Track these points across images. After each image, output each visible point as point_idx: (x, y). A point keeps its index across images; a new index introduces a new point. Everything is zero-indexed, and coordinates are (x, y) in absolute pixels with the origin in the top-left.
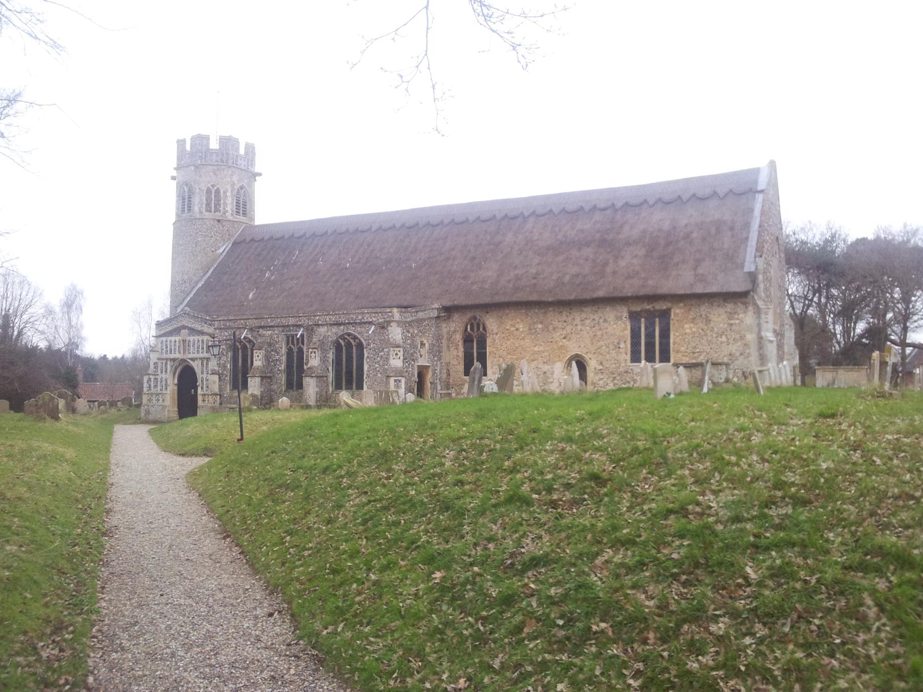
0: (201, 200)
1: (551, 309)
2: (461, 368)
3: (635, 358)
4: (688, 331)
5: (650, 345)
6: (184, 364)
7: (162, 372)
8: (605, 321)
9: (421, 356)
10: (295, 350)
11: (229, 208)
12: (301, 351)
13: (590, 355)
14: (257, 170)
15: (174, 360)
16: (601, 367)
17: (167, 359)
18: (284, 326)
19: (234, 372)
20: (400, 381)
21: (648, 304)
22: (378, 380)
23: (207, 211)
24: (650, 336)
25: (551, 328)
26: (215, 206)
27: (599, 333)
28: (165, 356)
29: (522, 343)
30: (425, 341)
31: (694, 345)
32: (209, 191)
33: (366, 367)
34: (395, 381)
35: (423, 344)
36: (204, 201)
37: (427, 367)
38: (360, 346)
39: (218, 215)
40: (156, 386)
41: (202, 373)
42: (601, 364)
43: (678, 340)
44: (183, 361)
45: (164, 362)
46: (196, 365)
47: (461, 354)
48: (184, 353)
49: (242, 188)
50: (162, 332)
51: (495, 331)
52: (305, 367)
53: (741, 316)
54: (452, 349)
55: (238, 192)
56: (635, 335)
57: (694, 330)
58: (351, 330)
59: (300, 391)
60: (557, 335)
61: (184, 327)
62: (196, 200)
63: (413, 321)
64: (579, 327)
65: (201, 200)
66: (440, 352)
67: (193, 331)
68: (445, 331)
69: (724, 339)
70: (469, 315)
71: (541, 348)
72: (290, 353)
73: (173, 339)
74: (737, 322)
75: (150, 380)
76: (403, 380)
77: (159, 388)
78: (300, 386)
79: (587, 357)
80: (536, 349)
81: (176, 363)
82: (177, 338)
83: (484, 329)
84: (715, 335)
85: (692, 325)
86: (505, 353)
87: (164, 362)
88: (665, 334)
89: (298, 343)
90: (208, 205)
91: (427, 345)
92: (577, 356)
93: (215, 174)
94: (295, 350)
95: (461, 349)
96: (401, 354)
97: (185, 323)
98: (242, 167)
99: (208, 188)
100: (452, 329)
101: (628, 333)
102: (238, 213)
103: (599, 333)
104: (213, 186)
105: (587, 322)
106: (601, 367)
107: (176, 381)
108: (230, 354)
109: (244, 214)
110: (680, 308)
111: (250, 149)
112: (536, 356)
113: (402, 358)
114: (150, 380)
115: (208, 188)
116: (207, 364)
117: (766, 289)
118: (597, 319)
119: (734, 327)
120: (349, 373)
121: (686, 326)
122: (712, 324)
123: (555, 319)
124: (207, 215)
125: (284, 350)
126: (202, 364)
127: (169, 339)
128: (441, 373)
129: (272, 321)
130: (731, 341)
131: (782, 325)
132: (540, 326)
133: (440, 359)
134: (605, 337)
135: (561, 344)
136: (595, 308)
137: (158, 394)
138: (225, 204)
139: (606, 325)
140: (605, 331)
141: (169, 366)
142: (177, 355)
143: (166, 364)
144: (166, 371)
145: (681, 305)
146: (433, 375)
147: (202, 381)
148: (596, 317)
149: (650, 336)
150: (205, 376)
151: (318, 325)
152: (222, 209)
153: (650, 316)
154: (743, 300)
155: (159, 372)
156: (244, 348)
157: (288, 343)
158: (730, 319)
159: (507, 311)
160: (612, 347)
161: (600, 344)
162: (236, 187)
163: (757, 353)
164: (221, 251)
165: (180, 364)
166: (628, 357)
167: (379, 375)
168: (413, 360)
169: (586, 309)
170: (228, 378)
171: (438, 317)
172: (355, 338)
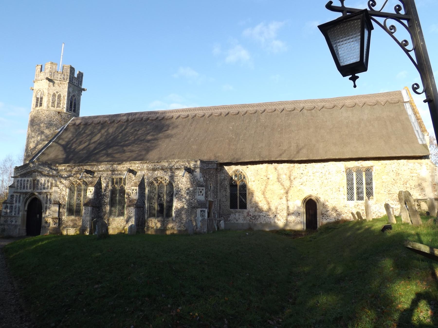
0: (49, 100)
2: (228, 203)
3: (351, 198)
6: (33, 197)
7: (16, 202)
11: (65, 106)
14: (83, 87)
15: (26, 193)
17: (20, 193)
20: (204, 211)
23: (52, 106)
24: (360, 183)
26: (58, 104)
31: (389, 189)
32: (54, 95)
34: (201, 211)
36: (51, 101)
45: (18, 194)
47: (228, 194)
48: (34, 189)
49: (74, 96)
54: (222, 191)
55: (72, 98)
65: (49, 100)
66: (217, 193)
82: (30, 179)
87: (18, 194)
90: (53, 103)
93: (59, 85)
95: (228, 190)
98: (75, 84)
99: (54, 94)
100: (223, 178)
104: (57, 92)
107: (26, 208)
109: (74, 111)
111: (81, 75)
113: (204, 194)
115: (54, 94)
122: (400, 176)
133: (217, 197)
138: (64, 103)
141: (21, 198)
142: (29, 190)
143: (20, 196)
144: (19, 201)
149: (360, 183)
152: (61, 106)
153: (359, 171)
155: (14, 202)
158: (411, 173)
162: (71, 95)
165: (30, 197)
166: (346, 197)
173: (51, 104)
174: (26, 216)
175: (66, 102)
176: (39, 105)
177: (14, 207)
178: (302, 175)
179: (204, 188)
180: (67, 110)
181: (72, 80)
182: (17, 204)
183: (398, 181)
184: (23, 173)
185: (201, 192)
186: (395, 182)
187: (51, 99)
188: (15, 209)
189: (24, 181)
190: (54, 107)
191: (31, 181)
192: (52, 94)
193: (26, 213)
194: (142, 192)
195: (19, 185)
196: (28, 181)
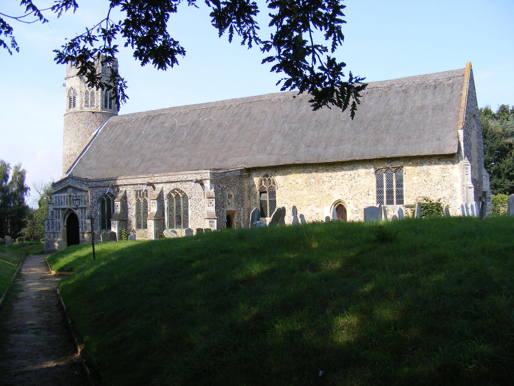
0: (82, 99)
1: (321, 168)
4: (415, 182)
5: (390, 192)
6: (70, 212)
7: (56, 218)
8: (359, 176)
9: (229, 204)
10: (142, 201)
11: (99, 104)
12: (146, 202)
13: (348, 201)
15: (63, 209)
16: (356, 209)
17: (59, 209)
18: (134, 185)
19: (102, 217)
21: (388, 164)
22: (199, 221)
23: (86, 106)
24: (390, 185)
25: (321, 181)
26: (91, 103)
27: (355, 184)
28: (58, 207)
29: (301, 192)
30: (232, 193)
31: (419, 191)
33: (190, 212)
35: (230, 196)
37: (233, 213)
38: (185, 197)
39: (93, 109)
40: (53, 228)
41: (82, 218)
42: (357, 206)
43: (408, 189)
44: (70, 210)
46: (77, 212)
50: (56, 190)
51: (282, 185)
52: (149, 213)
53: (450, 170)
54: (252, 198)
56: (379, 185)
57: (419, 181)
58: (179, 186)
59: (146, 230)
60: (325, 187)
61: (70, 187)
62: (78, 99)
63: (222, 178)
64: (341, 181)
65: (82, 99)
67: (75, 188)
68: (246, 185)
69: (439, 187)
70: (264, 173)
71: (314, 197)
72: (138, 204)
73: (63, 195)
74: (448, 174)
75: (49, 223)
76: (216, 221)
77: (55, 229)
78: (146, 227)
79: (346, 202)
80: (311, 197)
81: (65, 211)
82: (66, 195)
83: (274, 183)
84: (433, 185)
85: (418, 178)
86: (289, 200)
88: (400, 184)
89: (143, 196)
90: (86, 102)
91: (233, 196)
92: (339, 201)
94: (142, 201)
96: (214, 203)
97: (70, 184)
99: (87, 91)
101: (374, 184)
102: (106, 107)
103: (355, 184)
105: (346, 177)
106: (356, 209)
107: (65, 224)
108: (99, 205)
110: (410, 165)
112: (311, 202)
114: (49, 223)
116: (85, 212)
117: (466, 152)
118: (353, 175)
119: (446, 178)
120: (178, 217)
121: (414, 178)
122: (431, 177)
123: (324, 175)
124: (87, 109)
125: (134, 201)
126: (82, 212)
127: (60, 195)
128: (243, 215)
129: (126, 182)
130: (444, 188)
131: (480, 176)
132: (313, 180)
133: (243, 206)
134: (359, 187)
135: (328, 193)
136: (351, 167)
137: (54, 233)
138: (97, 100)
139: (359, 179)
140: (358, 183)
141: (60, 214)
142: (66, 206)
143: (59, 212)
144: (59, 217)
145: (410, 163)
146: (238, 217)
147: (82, 224)
148: (352, 172)
149: (390, 185)
150: (83, 220)
151: (157, 183)
152: (95, 104)
154: (452, 159)
155: (55, 218)
156: (109, 200)
157: (137, 197)
159: (290, 170)
160: (363, 194)
161: (356, 192)
163: (461, 197)
164: (95, 133)
165: (68, 212)
167: (199, 218)
168: (223, 207)
169: (345, 168)
170: (98, 222)
171: (241, 176)
172: (181, 192)
173: (84, 103)
174: (66, 231)
175: (100, 100)
176: (72, 106)
177: (55, 223)
178: (331, 179)
179: (214, 200)
180: (102, 108)
181: (105, 71)
182: (58, 220)
183: (429, 182)
184: (59, 189)
185: (211, 203)
186: (425, 183)
187: (84, 98)
188: (56, 225)
189: (61, 196)
190: (88, 107)
191: (67, 197)
192: (85, 91)
193: (66, 228)
194: (161, 204)
195: (57, 201)
196: (64, 197)
